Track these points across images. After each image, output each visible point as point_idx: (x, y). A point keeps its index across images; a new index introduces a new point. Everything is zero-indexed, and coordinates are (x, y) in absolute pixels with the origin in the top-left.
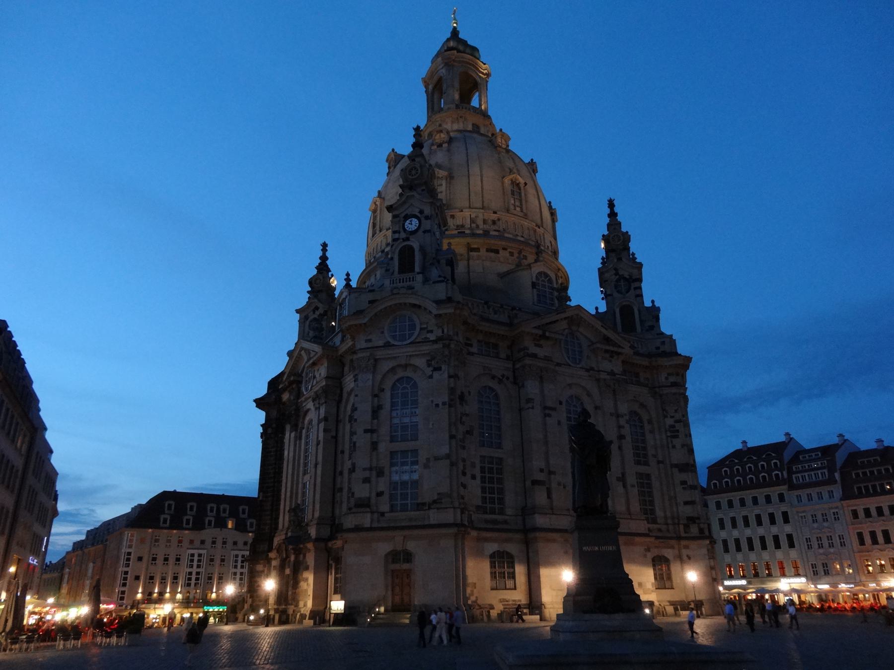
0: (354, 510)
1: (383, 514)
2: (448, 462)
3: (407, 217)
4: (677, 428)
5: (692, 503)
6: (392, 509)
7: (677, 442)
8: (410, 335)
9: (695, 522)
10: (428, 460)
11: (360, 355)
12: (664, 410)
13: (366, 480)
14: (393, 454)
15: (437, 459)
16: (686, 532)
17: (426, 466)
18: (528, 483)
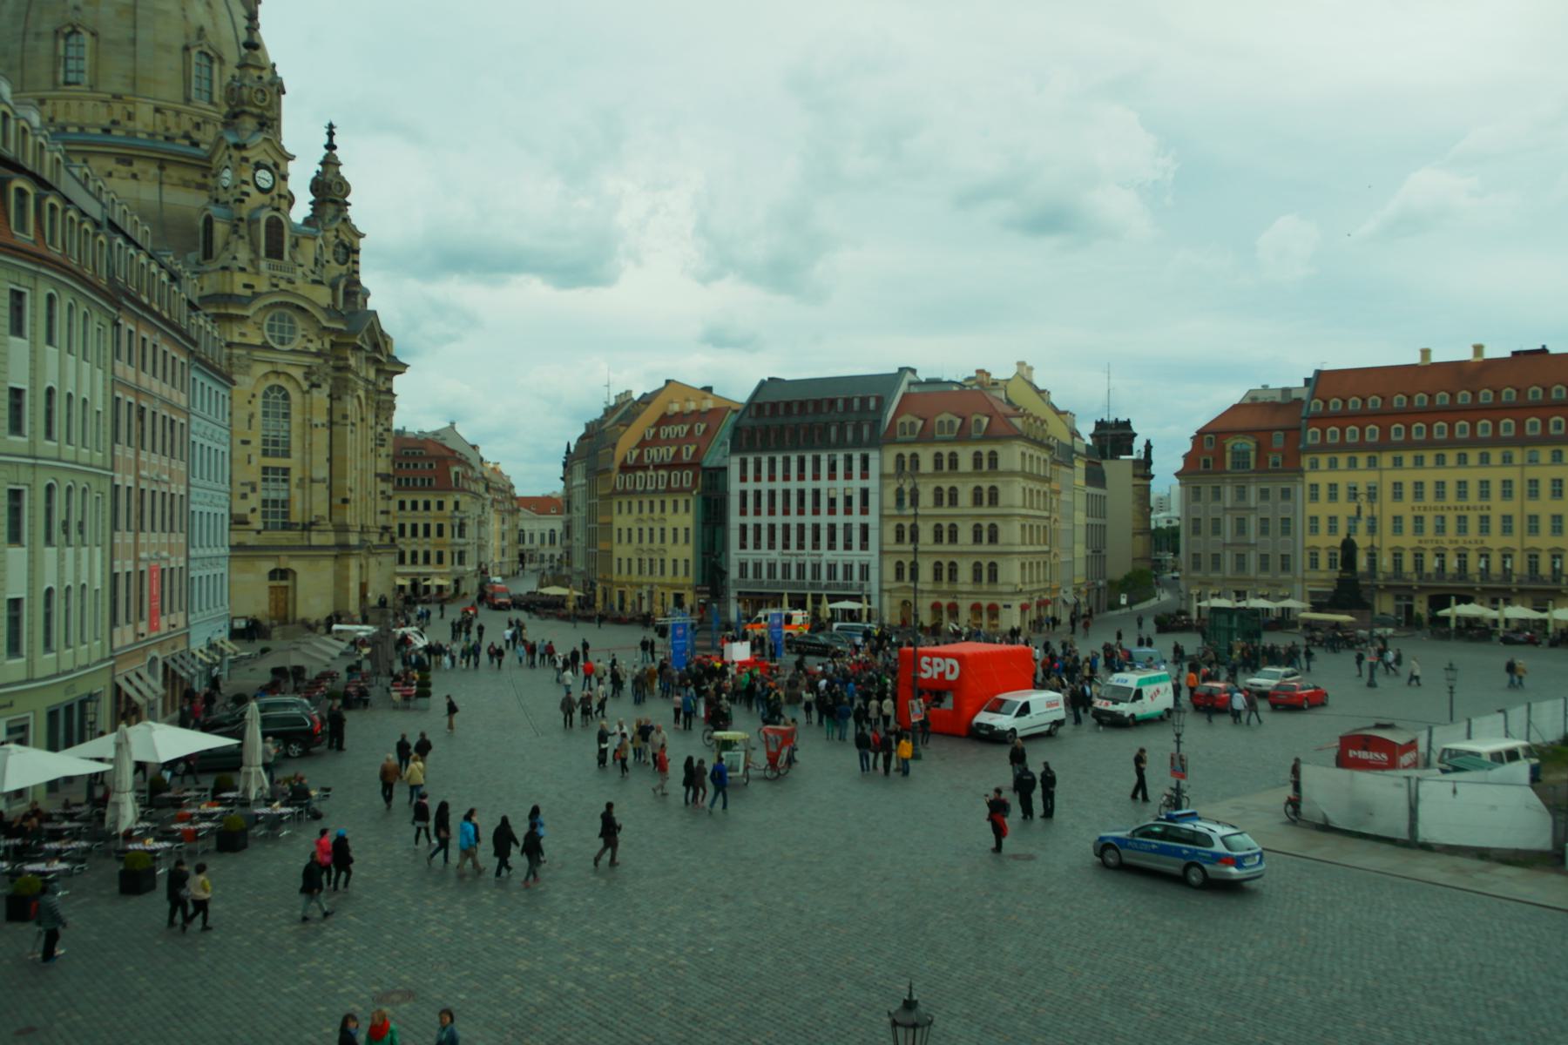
1: (259, 532)
3: (258, 166)
6: (266, 528)
7: (383, 451)
8: (291, 339)
10: (302, 480)
11: (237, 351)
13: (244, 496)
14: (265, 470)
15: (312, 481)
17: (298, 486)
18: (337, 501)
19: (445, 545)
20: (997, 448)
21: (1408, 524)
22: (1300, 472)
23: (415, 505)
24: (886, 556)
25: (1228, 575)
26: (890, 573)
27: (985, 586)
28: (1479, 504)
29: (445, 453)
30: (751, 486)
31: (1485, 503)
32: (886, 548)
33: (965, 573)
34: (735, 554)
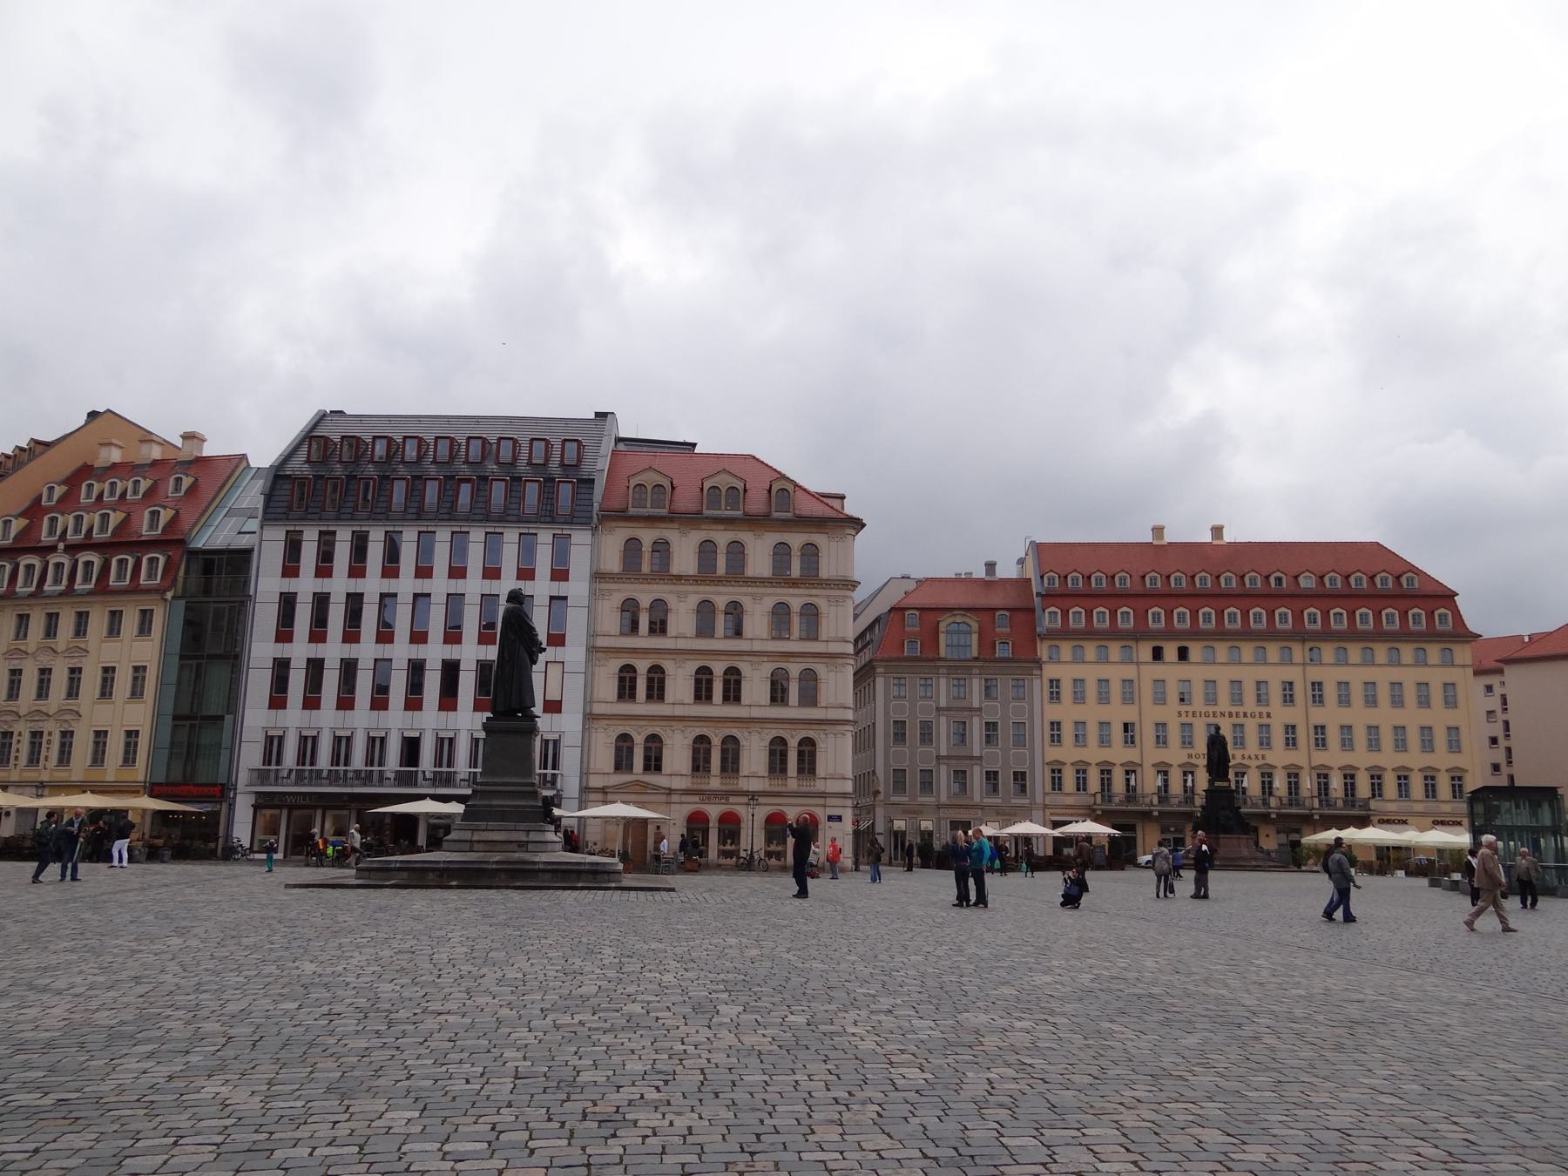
20: (819, 539)
21: (1174, 735)
22: (1038, 663)
24: (595, 724)
25: (944, 799)
26: (604, 757)
27: (793, 784)
28: (1258, 710)
30: (306, 585)
31: (1264, 710)
32: (598, 709)
33: (754, 757)
34: (256, 717)
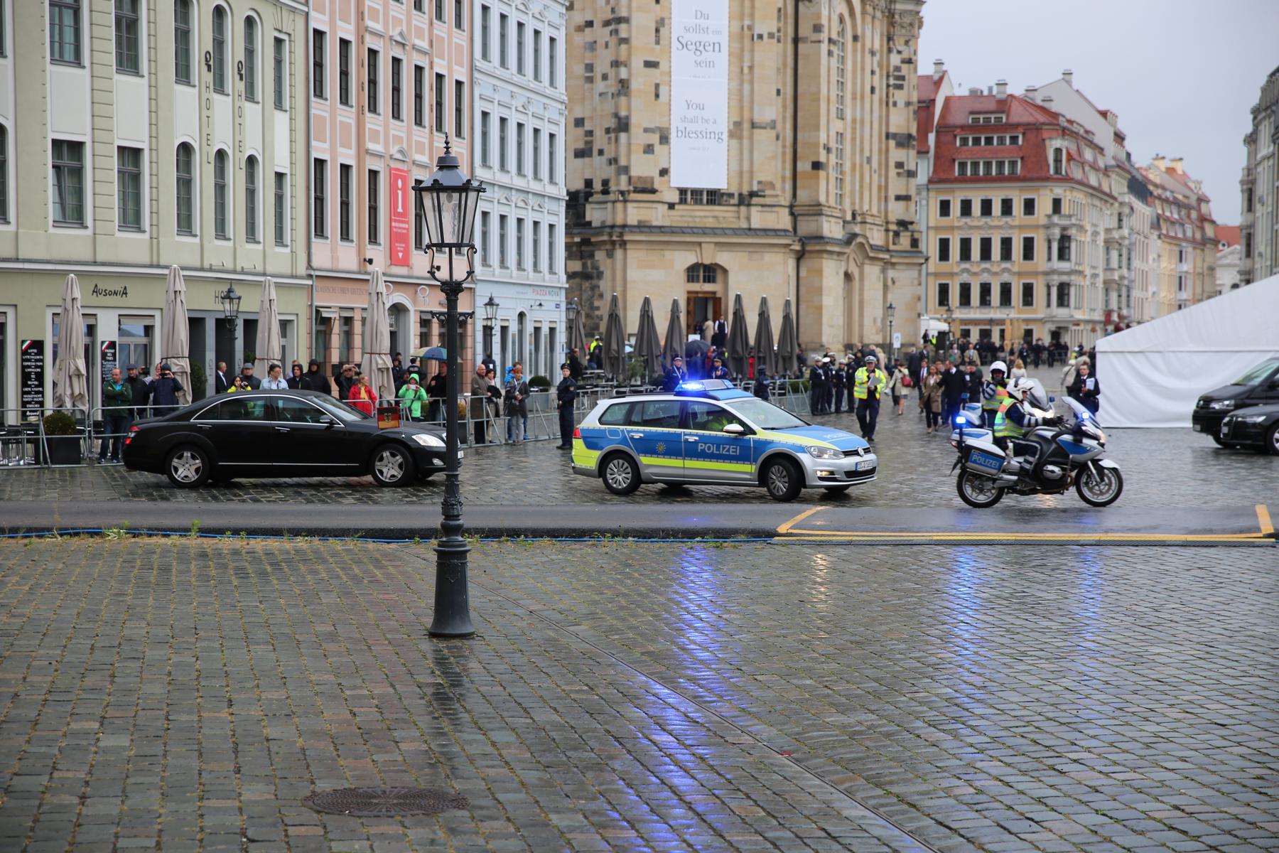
0: (633, 196)
1: (671, 206)
2: (773, 133)
4: (903, 73)
5: (907, 198)
6: (683, 201)
7: (900, 97)
9: (907, 229)
12: (889, 39)
13: (649, 149)
15: (753, 126)
16: (894, 244)
19: (1036, 274)
23: (987, 207)
29: (1042, 118)
